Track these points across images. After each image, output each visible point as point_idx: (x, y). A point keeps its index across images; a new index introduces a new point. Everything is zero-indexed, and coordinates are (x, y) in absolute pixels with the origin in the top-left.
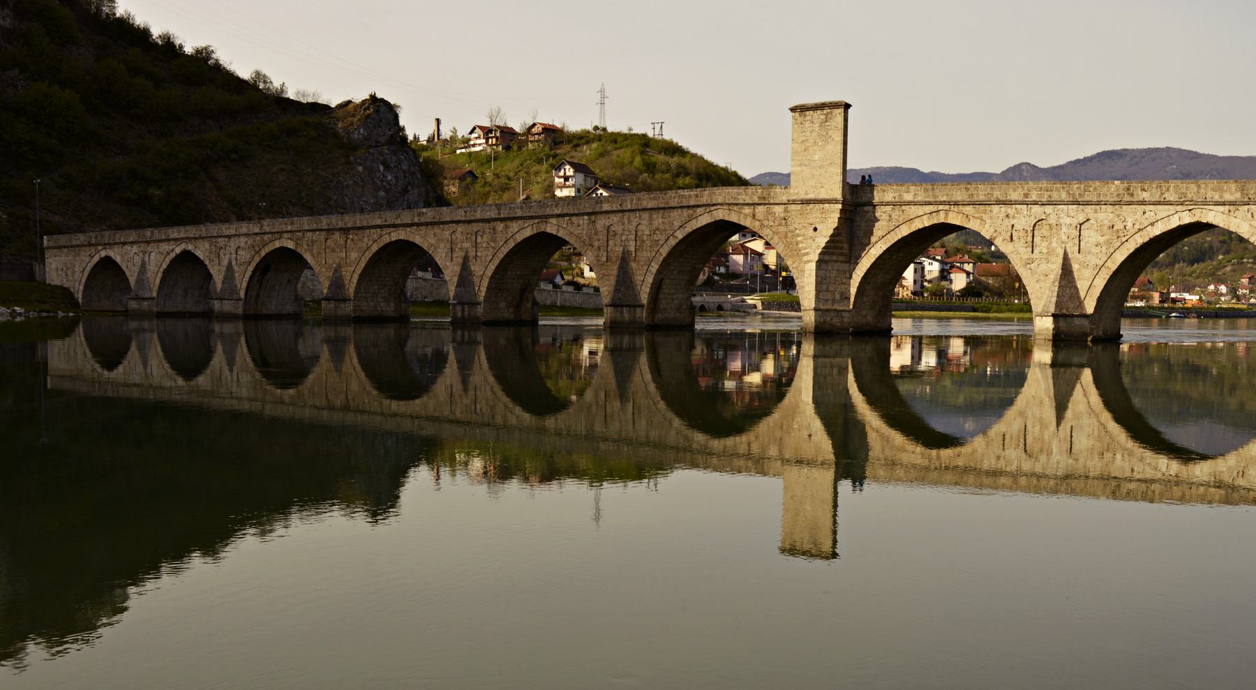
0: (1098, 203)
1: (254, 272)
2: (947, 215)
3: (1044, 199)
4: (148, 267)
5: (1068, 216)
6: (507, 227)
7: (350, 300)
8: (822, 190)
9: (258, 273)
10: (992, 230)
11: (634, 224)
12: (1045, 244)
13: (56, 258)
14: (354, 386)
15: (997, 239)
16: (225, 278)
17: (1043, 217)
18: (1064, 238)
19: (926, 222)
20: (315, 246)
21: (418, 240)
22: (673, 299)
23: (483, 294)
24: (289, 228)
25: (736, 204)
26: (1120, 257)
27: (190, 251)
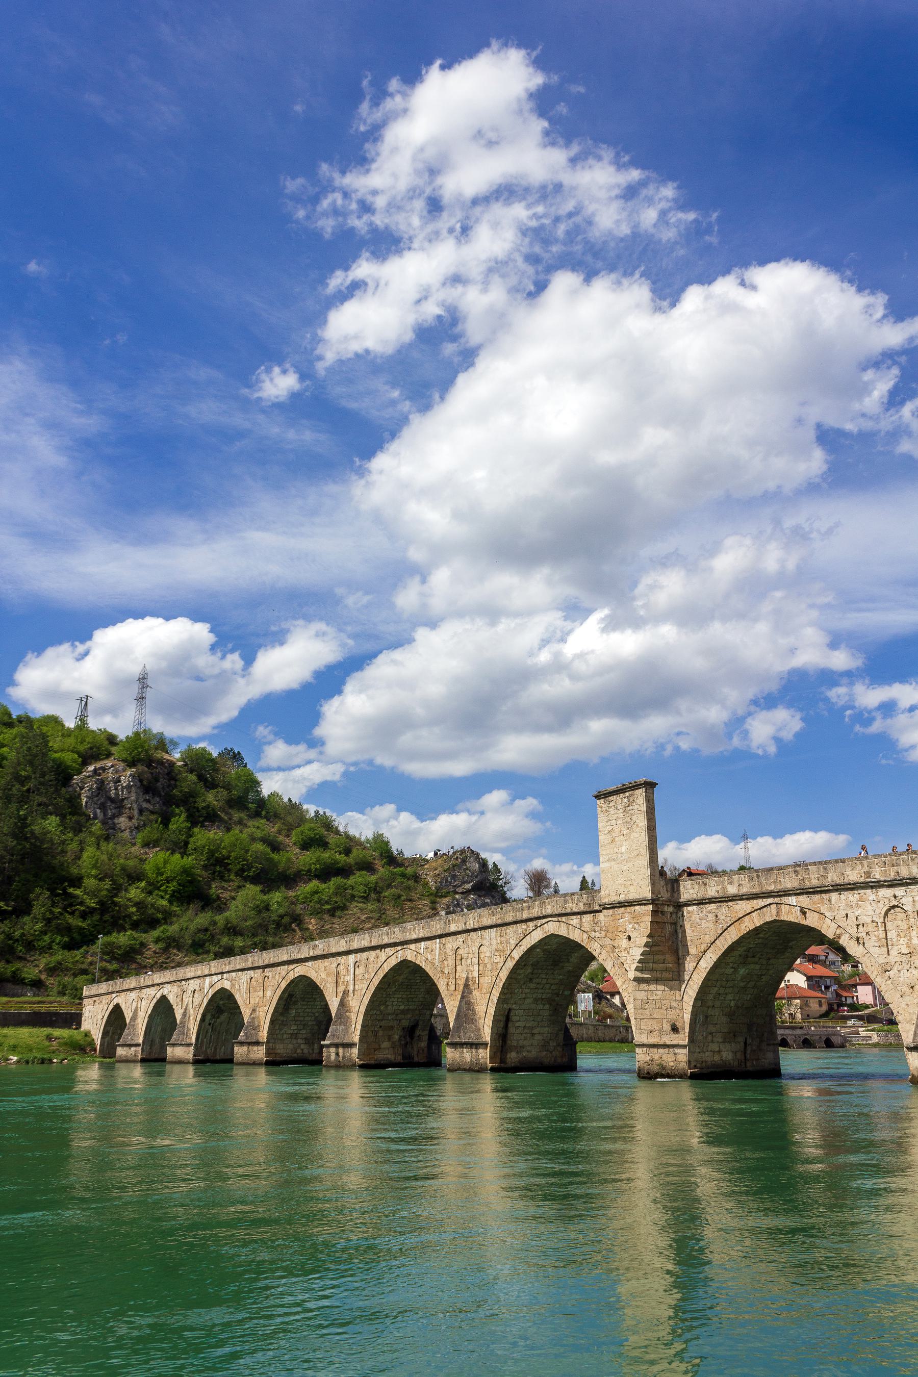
2: (778, 912)
8: (632, 889)
9: (208, 1017)
12: (903, 941)
15: (842, 938)
17: (894, 903)
22: (533, 1034)
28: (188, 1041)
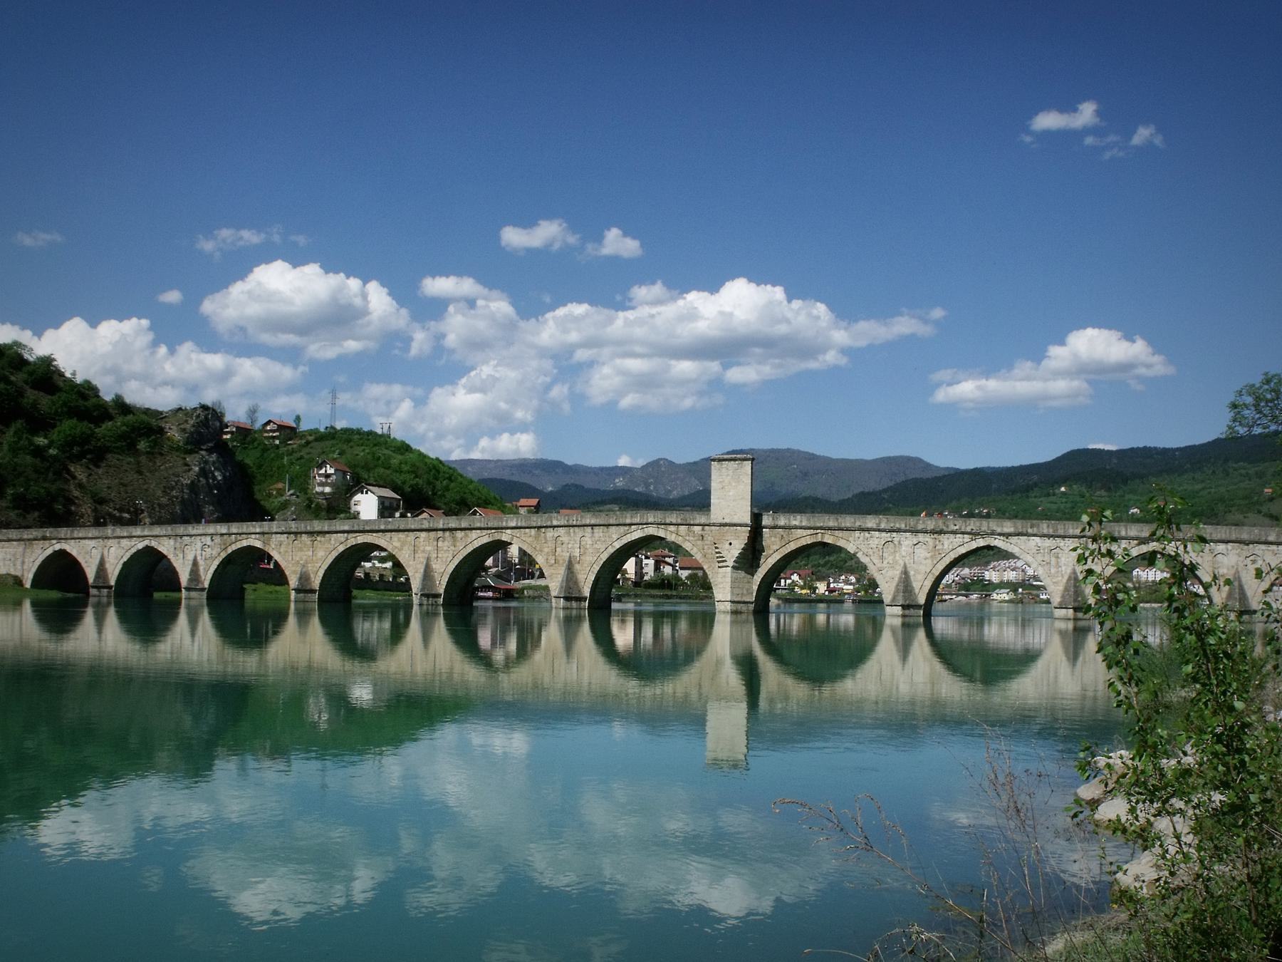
12: (891, 558)
19: (809, 541)
24: (258, 530)
27: (152, 548)
28: (200, 586)
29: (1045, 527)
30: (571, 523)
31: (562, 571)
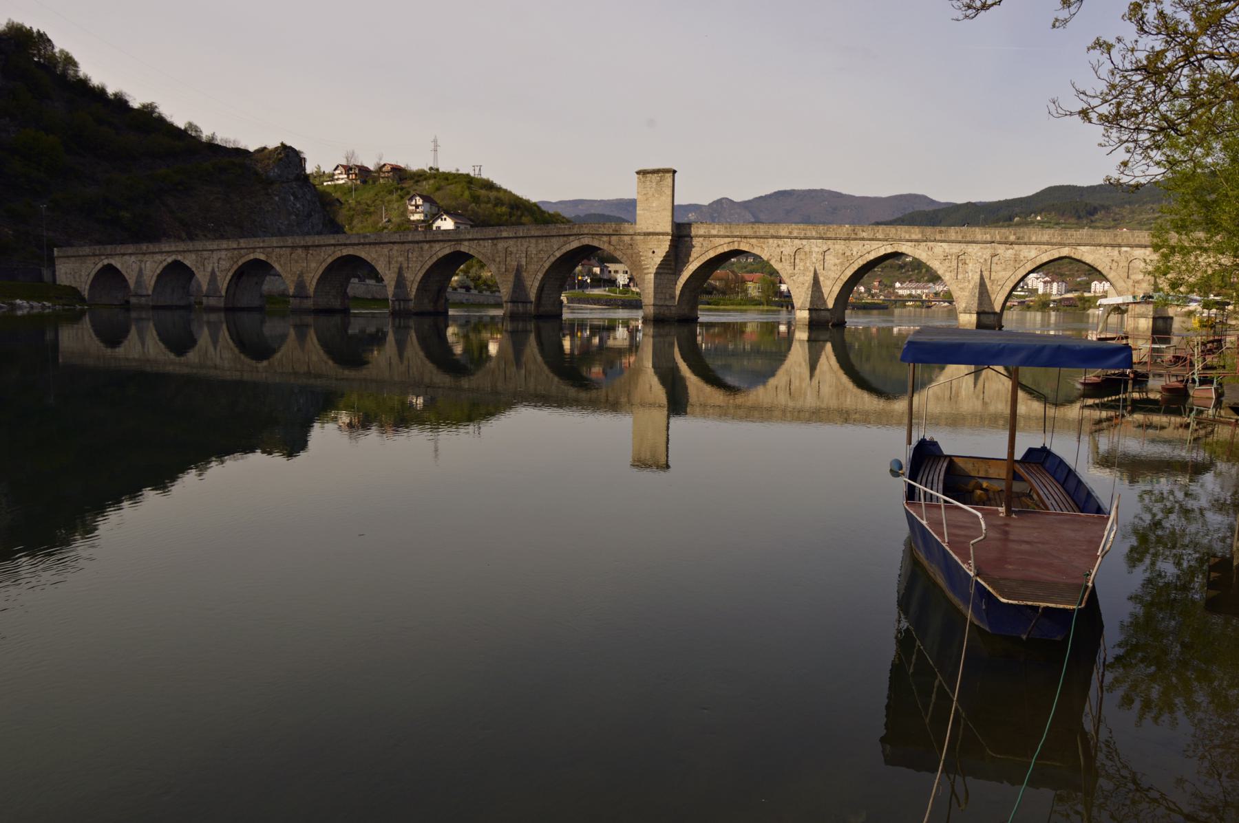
0: (836, 239)
1: (232, 277)
3: (802, 236)
4: (144, 272)
5: (816, 247)
6: (431, 247)
7: (310, 297)
10: (769, 254)
11: (525, 246)
12: (802, 264)
13: (66, 265)
14: (315, 358)
16: (210, 281)
17: (801, 247)
18: (814, 260)
19: (726, 249)
20: (283, 259)
21: (363, 255)
23: (414, 293)
24: (261, 245)
25: (597, 235)
26: (849, 273)
27: (179, 261)
29: (953, 233)
30: (518, 235)
31: (511, 278)
